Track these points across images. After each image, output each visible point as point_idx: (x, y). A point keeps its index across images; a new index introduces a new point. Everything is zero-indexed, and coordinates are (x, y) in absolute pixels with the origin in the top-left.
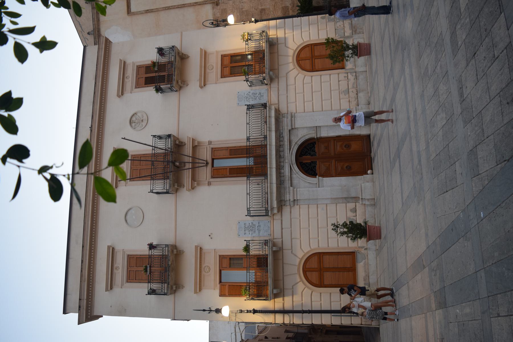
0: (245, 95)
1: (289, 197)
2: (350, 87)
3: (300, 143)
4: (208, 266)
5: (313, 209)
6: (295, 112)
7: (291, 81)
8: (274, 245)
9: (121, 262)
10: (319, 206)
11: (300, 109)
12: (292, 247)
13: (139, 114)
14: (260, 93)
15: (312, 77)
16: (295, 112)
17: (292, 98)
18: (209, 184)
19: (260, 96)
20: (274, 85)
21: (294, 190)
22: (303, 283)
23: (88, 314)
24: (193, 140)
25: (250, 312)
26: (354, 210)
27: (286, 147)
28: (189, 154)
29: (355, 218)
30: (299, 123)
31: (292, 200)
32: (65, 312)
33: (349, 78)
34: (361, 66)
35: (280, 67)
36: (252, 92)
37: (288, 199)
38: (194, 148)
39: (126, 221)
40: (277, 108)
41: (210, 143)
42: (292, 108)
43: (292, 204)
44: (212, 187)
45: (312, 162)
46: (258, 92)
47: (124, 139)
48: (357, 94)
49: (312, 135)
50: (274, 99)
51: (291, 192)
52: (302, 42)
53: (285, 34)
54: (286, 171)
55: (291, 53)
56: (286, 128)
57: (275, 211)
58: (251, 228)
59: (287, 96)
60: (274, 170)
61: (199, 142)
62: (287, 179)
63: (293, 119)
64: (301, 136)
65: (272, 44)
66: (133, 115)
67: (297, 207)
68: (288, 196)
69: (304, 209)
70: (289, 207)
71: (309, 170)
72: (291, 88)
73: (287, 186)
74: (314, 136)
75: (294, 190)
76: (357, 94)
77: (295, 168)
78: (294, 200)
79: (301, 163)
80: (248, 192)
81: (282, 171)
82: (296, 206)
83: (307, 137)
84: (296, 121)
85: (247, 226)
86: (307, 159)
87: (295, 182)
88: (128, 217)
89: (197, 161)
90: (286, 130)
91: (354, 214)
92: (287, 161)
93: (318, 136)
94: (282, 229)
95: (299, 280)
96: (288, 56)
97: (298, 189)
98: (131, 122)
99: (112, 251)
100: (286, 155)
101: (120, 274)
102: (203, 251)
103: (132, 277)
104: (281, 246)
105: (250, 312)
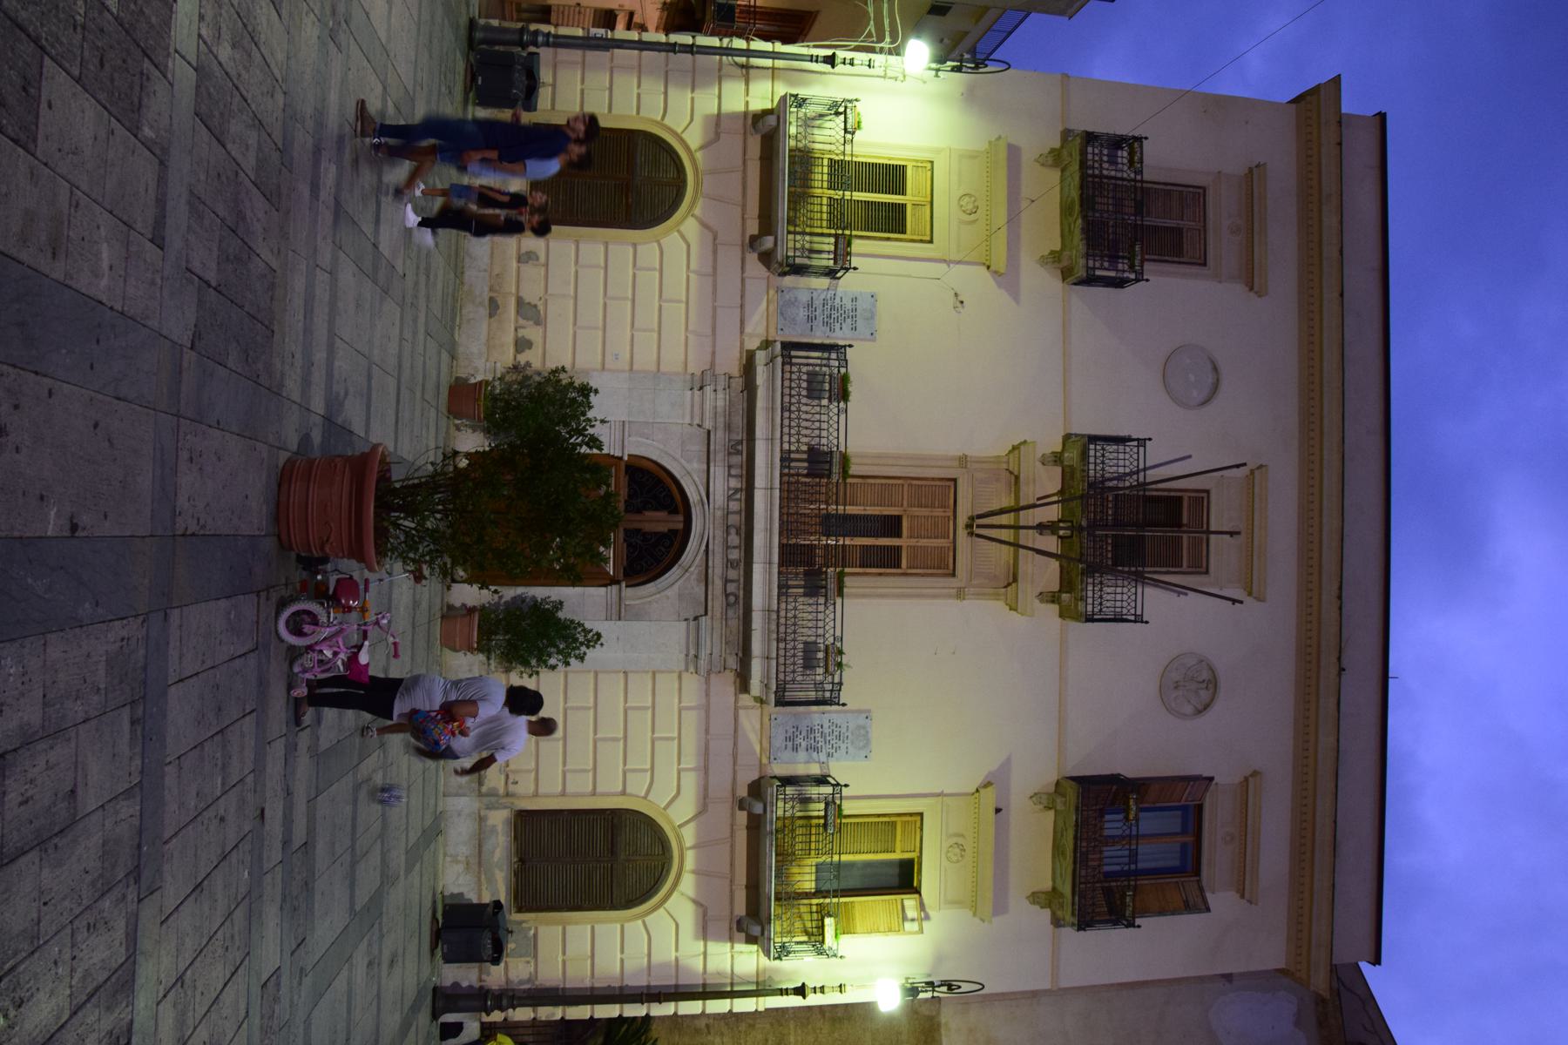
0: (844, 747)
1: (717, 399)
3: (675, 572)
5: (646, 360)
6: (685, 676)
7: (690, 783)
8: (766, 258)
9: (1223, 244)
10: (627, 367)
11: (667, 683)
12: (715, 252)
13: (1189, 709)
14: (795, 749)
15: (624, 793)
16: (685, 676)
17: (692, 721)
18: (963, 461)
19: (798, 741)
20: (748, 776)
22: (687, 148)
23: (1316, 106)
26: (522, 345)
29: (522, 322)
30: (676, 633)
31: (708, 389)
32: (1382, 117)
33: (503, 777)
36: (823, 757)
37: (720, 395)
39: (1215, 369)
41: (960, 594)
43: (708, 378)
44: (955, 450)
45: (639, 511)
46: (802, 755)
47: (1234, 601)
49: (634, 596)
50: (751, 721)
51: (707, 415)
52: (648, 919)
53: (705, 954)
55: (688, 884)
56: (717, 624)
57: (761, 357)
58: (834, 313)
59: (707, 731)
60: (760, 481)
62: (720, 456)
63: (692, 652)
64: (671, 592)
65: (751, 924)
66: (1206, 707)
67: (695, 368)
68: (720, 403)
69: (673, 358)
70: (720, 370)
71: (652, 486)
72: (690, 761)
73: (720, 434)
74: (628, 593)
78: (701, 388)
79: (673, 511)
80: (843, 417)
81: (734, 483)
82: (698, 373)
83: (650, 587)
84: (683, 641)
85: (849, 321)
86: (657, 522)
87: (698, 447)
88: (1210, 379)
90: (718, 615)
91: (521, 333)
93: (615, 588)
94: (742, 306)
95: (698, 155)
96: (695, 872)
97: (687, 420)
98: (1213, 684)
99: (1251, 278)
101: (1222, 213)
103: (1192, 197)
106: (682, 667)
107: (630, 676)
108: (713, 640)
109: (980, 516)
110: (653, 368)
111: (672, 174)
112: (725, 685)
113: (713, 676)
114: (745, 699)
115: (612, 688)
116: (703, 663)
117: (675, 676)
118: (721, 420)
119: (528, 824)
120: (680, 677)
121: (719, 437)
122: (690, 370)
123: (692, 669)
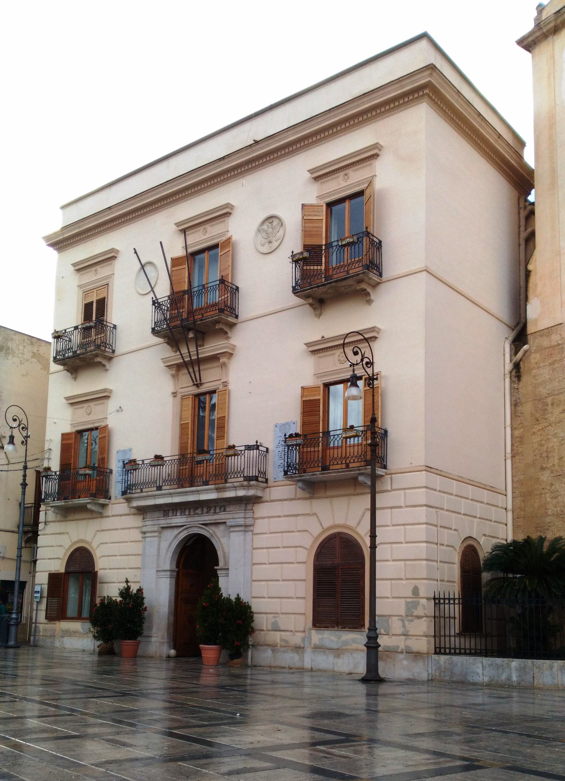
2: (282, 633)
4: (91, 411)
6: (255, 532)
11: (259, 541)
16: (255, 532)
18: (174, 394)
21: (155, 532)
23: (60, 243)
24: (230, 355)
25: (24, 480)
27: (211, 517)
28: (204, 353)
32: (63, 207)
34: (312, 660)
38: (215, 358)
40: (263, 499)
42: (260, 526)
44: (170, 399)
54: (178, 520)
61: (224, 365)
62: (169, 521)
63: (243, 528)
89: (196, 369)
92: (189, 520)
93: (219, 572)
100: (197, 519)
102: (105, 401)
104: (104, 515)
105: (24, 480)
106: (250, 533)
107: (254, 562)
108: (234, 516)
109: (193, 382)
110: (140, 557)
111: (78, 554)
112: (261, 510)
113: (256, 516)
114: (266, 497)
115: (260, 572)
116: (249, 521)
117: (255, 537)
118: (156, 522)
119: (320, 620)
120: (255, 534)
121: (163, 522)
122: (141, 539)
123: (251, 528)
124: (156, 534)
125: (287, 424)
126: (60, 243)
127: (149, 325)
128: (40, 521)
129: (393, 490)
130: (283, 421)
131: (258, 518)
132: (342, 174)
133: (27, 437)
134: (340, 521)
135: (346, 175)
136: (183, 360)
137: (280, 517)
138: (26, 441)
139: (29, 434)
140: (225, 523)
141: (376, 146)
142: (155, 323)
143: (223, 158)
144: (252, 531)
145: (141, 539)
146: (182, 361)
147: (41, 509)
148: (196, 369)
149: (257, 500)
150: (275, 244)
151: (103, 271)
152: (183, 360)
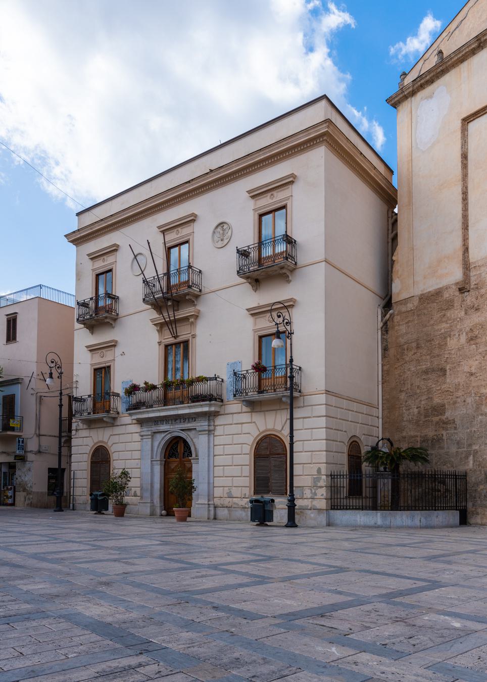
2: (234, 499)
16: (216, 434)
18: (160, 343)
21: (149, 435)
23: (78, 239)
24: (196, 317)
25: (61, 402)
26: (135, 495)
28: (177, 315)
33: (244, 499)
35: (262, 413)
38: (186, 319)
40: (221, 413)
42: (219, 430)
48: (227, 507)
56: (199, 424)
57: (135, 417)
62: (158, 428)
73: (153, 429)
75: (149, 435)
76: (227, 507)
77: (169, 436)
89: (174, 326)
92: (172, 427)
93: (192, 461)
100: (176, 426)
104: (115, 425)
105: (61, 402)
108: (202, 424)
112: (219, 421)
114: (222, 412)
116: (212, 428)
118: (150, 429)
123: (213, 432)
124: (150, 437)
125: (235, 363)
126: (78, 239)
127: (141, 297)
128: (73, 429)
129: (304, 406)
130: (233, 361)
131: (217, 426)
132: (269, 194)
133: (61, 373)
134: (270, 426)
135: (272, 195)
136: (165, 319)
137: (231, 424)
138: (61, 376)
139: (62, 371)
140: (195, 429)
141: (293, 176)
142: (145, 295)
143: (189, 182)
144: (214, 434)
145: (140, 440)
146: (164, 321)
147: (73, 421)
148: (174, 326)
149: (216, 414)
150: (226, 241)
151: (110, 259)
152: (165, 319)
